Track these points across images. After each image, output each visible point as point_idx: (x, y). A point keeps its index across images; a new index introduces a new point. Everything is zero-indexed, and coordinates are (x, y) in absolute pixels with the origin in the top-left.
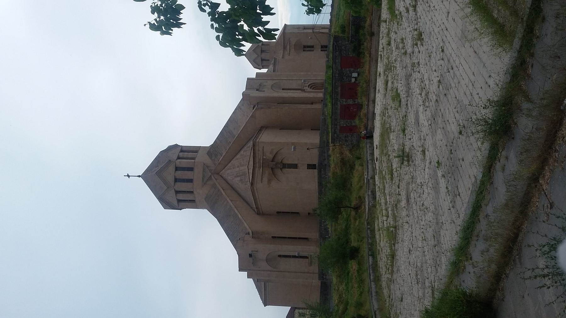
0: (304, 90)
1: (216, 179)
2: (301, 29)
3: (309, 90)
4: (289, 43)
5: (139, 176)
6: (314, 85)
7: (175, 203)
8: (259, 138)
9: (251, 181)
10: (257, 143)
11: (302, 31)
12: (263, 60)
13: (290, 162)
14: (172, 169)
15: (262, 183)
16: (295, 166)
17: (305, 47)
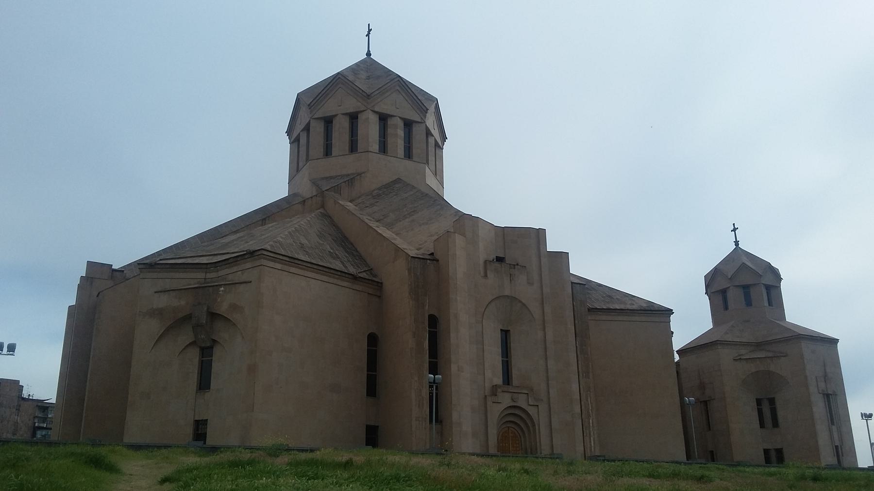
0: (496, 395)
1: (304, 201)
2: (822, 385)
3: (496, 411)
4: (770, 354)
5: (369, 54)
6: (526, 424)
7: (295, 135)
8: (293, 270)
9: (161, 262)
10: (258, 263)
11: (813, 389)
12: (724, 292)
13: (216, 367)
14: (351, 104)
15: (156, 292)
16: (204, 384)
17: (772, 401)
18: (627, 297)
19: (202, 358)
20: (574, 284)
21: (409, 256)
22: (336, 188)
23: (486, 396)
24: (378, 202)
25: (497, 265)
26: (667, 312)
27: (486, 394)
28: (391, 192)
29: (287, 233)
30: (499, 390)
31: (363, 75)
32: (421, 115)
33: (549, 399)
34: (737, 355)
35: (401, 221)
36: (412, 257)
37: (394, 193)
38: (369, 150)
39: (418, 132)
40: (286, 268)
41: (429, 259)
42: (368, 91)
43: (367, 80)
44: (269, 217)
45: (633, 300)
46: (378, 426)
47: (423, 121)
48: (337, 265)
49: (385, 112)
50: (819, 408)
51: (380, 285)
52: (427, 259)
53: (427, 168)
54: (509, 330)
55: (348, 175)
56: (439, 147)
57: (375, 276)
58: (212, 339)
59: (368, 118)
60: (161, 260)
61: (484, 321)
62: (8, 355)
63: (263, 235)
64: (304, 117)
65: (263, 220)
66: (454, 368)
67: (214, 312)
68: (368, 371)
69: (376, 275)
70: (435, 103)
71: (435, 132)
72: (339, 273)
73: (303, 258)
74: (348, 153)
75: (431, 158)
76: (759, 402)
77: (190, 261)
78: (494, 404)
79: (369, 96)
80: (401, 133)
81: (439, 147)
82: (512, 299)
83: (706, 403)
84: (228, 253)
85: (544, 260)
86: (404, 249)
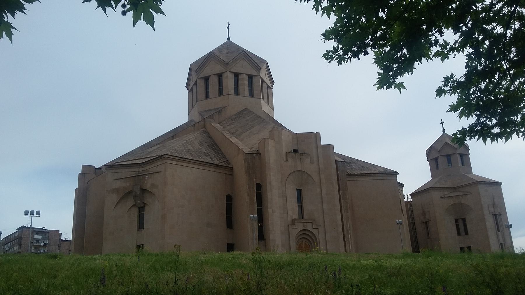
0: (294, 224)
1: (194, 125)
2: (492, 209)
3: (294, 232)
4: (461, 194)
5: (229, 39)
8: (183, 164)
10: (164, 162)
11: (486, 212)
12: (436, 159)
13: (146, 217)
14: (218, 69)
15: (114, 180)
16: (141, 226)
17: (464, 220)
18: (373, 166)
19: (140, 212)
20: (338, 162)
21: (244, 152)
22: (211, 116)
23: (288, 225)
24: (234, 122)
25: (293, 154)
26: (395, 174)
27: (289, 224)
28: (241, 117)
29: (181, 144)
30: (296, 221)
31: (225, 52)
32: (257, 72)
33: (324, 225)
34: (442, 195)
35: (244, 133)
36: (246, 153)
37: (243, 117)
38: (229, 94)
39: (256, 82)
40: (179, 163)
41: (255, 154)
42: (227, 61)
43: (227, 55)
44: (175, 135)
45: (376, 168)
46: (234, 244)
47: (259, 75)
48: (208, 160)
49: (237, 72)
50: (490, 222)
51: (232, 169)
52: (254, 154)
53: (262, 101)
54: (301, 189)
55: (218, 108)
56: (270, 88)
57: (229, 164)
58: (144, 203)
59: (228, 76)
60: (116, 163)
61: (286, 185)
62: (37, 216)
63: (170, 145)
64: (194, 78)
65: (172, 136)
66: (270, 211)
67: (143, 188)
68: (227, 215)
69: (230, 164)
70: (266, 64)
71: (267, 81)
72: (208, 164)
73: (188, 157)
74: (218, 96)
75: (265, 95)
76: (457, 221)
77: (130, 162)
78: (293, 229)
79: (227, 63)
80: (246, 83)
81: (269, 88)
82: (302, 172)
83: (426, 223)
84: (151, 157)
85: (320, 150)
86: (242, 149)
